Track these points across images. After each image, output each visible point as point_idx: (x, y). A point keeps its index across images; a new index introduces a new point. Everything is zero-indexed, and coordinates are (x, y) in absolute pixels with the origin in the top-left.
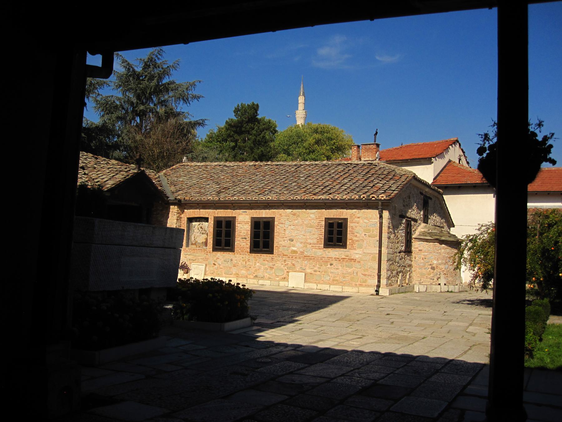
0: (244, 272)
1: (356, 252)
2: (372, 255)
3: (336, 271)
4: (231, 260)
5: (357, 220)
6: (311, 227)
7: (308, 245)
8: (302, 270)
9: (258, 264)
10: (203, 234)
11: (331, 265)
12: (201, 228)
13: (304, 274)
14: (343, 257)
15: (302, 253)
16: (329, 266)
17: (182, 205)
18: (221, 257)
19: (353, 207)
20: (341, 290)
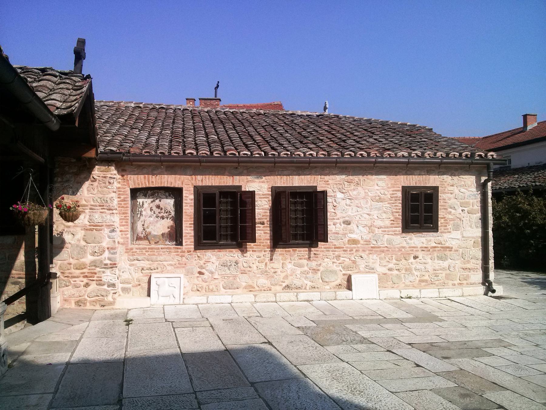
0: (263, 281)
1: (451, 236)
2: (473, 240)
3: (422, 267)
4: (237, 263)
5: (451, 188)
6: (380, 200)
7: (376, 229)
8: (370, 270)
9: (290, 266)
10: (163, 218)
11: (415, 257)
12: (158, 207)
13: (376, 276)
14: (435, 245)
15: (368, 242)
16: (412, 260)
17: (123, 162)
18: (213, 259)
19: (443, 170)
20: (437, 295)
